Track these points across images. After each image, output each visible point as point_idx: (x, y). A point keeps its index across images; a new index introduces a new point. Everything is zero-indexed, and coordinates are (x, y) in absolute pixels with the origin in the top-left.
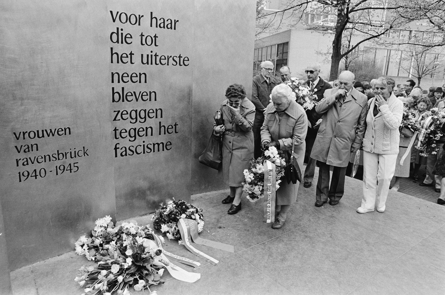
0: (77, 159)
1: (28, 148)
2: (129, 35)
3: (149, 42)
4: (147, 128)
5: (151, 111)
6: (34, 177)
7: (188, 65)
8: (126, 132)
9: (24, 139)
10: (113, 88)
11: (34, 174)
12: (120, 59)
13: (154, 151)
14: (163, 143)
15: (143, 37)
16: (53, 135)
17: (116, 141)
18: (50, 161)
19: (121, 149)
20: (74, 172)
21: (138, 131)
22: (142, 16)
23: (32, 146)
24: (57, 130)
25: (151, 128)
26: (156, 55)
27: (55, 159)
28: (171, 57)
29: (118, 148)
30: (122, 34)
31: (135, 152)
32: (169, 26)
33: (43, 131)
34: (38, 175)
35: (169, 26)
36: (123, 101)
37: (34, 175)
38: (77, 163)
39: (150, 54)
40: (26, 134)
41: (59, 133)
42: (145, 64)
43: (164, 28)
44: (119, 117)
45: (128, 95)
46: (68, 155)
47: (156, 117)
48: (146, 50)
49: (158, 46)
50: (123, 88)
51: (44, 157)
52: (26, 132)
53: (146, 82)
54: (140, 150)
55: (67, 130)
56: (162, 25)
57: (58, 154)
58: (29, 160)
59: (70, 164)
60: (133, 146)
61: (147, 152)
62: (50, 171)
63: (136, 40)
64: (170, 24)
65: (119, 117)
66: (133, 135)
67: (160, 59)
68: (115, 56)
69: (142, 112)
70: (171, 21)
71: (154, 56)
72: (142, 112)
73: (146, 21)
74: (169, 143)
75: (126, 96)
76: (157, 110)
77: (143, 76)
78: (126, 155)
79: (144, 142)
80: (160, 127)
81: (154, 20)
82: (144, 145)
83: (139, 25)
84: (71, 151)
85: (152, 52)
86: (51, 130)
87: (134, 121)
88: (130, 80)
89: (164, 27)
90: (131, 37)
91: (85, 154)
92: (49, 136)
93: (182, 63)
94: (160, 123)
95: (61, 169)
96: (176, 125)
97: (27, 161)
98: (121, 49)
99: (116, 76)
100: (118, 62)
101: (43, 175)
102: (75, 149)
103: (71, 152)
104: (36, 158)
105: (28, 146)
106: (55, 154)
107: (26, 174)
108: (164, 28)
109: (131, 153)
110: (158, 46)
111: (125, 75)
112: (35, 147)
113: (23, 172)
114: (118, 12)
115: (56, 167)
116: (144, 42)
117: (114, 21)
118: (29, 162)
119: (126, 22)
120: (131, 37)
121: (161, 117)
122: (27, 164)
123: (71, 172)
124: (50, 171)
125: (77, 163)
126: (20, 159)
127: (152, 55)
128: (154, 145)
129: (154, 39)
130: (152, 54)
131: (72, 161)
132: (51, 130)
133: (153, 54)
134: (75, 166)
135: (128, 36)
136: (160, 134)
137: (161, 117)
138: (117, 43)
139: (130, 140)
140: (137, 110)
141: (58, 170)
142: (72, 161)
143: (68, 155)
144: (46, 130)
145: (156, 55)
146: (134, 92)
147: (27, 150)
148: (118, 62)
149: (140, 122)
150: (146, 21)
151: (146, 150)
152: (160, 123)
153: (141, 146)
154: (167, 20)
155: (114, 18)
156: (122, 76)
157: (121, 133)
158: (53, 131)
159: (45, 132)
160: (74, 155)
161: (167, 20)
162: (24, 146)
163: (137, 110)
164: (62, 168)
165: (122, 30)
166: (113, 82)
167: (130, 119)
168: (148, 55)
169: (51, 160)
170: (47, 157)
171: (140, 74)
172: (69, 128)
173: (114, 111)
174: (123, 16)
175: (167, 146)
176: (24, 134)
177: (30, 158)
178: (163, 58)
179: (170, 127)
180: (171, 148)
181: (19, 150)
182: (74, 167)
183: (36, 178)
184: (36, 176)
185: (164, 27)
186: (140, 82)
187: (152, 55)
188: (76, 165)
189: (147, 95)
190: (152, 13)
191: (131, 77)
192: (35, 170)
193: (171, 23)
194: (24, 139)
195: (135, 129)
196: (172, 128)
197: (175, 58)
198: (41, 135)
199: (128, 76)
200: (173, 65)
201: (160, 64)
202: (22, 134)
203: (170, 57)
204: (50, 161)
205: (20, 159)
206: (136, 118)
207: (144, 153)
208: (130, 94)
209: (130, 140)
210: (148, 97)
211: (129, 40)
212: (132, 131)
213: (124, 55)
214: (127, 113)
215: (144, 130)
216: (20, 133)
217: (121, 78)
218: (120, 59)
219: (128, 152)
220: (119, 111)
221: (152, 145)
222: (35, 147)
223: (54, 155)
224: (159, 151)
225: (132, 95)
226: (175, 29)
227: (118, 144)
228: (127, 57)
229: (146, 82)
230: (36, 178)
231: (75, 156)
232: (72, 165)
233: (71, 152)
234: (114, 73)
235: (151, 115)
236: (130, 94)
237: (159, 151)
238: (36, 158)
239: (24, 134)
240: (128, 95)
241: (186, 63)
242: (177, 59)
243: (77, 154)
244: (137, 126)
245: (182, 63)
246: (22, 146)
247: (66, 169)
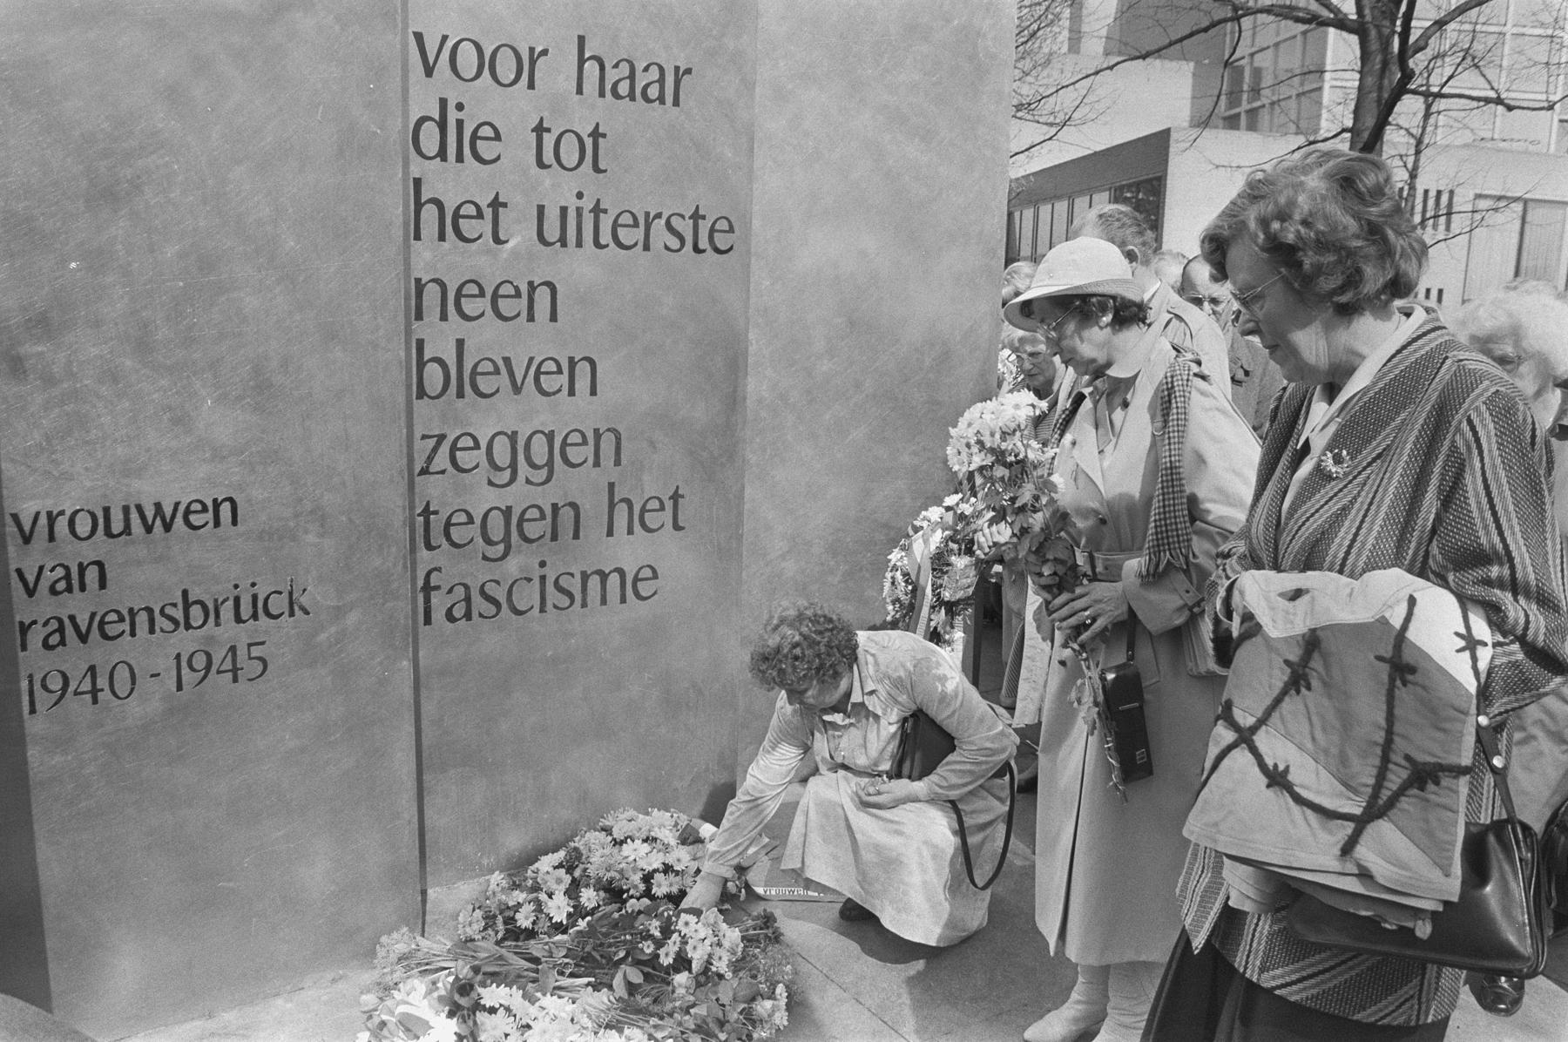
1: (68, 577)
2: (487, 128)
3: (570, 156)
5: (575, 438)
6: (88, 697)
7: (731, 248)
8: (471, 520)
9: (52, 538)
10: (420, 344)
11: (86, 686)
12: (452, 224)
13: (584, 605)
14: (621, 572)
15: (545, 135)
16: (167, 527)
18: (152, 631)
19: (450, 591)
20: (249, 680)
21: (521, 520)
22: (545, 52)
23: (82, 569)
24: (182, 508)
25: (573, 505)
26: (597, 210)
27: (169, 626)
28: (659, 216)
29: (437, 588)
30: (460, 123)
31: (505, 606)
32: (653, 92)
33: (126, 510)
34: (102, 690)
35: (653, 92)
36: (460, 394)
37: (90, 689)
38: (263, 643)
39: (572, 203)
40: (60, 518)
41: (192, 518)
42: (554, 244)
43: (633, 98)
44: (442, 460)
45: (479, 370)
46: (227, 611)
47: (597, 464)
48: (559, 190)
49: (605, 171)
50: (460, 344)
51: (127, 618)
52: (62, 513)
53: (554, 318)
54: (527, 596)
55: (226, 509)
56: (623, 89)
57: (187, 606)
58: (67, 622)
59: (233, 649)
60: (498, 582)
61: (555, 607)
62: (152, 676)
63: (517, 150)
64: (657, 85)
65: (442, 460)
66: (497, 533)
67: (615, 225)
68: (429, 213)
69: (540, 445)
70: (661, 69)
71: (590, 212)
72: (540, 445)
73: (557, 74)
74: (647, 573)
75: (474, 373)
77: (543, 296)
78: (468, 616)
79: (543, 564)
80: (612, 506)
81: (591, 68)
82: (543, 578)
83: (531, 86)
84: (236, 592)
85: (580, 196)
86: (158, 506)
87: (507, 474)
89: (632, 97)
90: (498, 137)
91: (296, 608)
92: (149, 529)
94: (611, 486)
95: (195, 666)
96: (676, 497)
97: (61, 629)
99: (432, 294)
100: (442, 237)
101: (122, 686)
102: (253, 585)
103: (237, 600)
104: (97, 619)
105: (67, 568)
106: (175, 605)
107: (56, 684)
108: (633, 98)
110: (605, 171)
112: (92, 575)
113: (45, 676)
114: (445, 38)
115: (178, 657)
117: (429, 71)
118: (67, 632)
119: (479, 74)
120: (498, 137)
121: (618, 462)
122: (63, 642)
123: (235, 680)
124: (152, 676)
125: (263, 643)
126: (34, 622)
127: (579, 211)
128: (585, 577)
129: (589, 142)
130: (580, 203)
132: (158, 506)
133: (587, 204)
134: (252, 655)
135: (486, 131)
136: (610, 533)
137: (618, 462)
138: (439, 159)
139: (485, 558)
140: (515, 433)
141: (183, 672)
142: (239, 635)
143: (227, 611)
144: (139, 508)
145: (597, 210)
146: (507, 360)
147: (61, 586)
148: (442, 237)
149: (528, 481)
150: (557, 74)
151: (553, 596)
152: (611, 486)
153: (529, 580)
154: (646, 69)
155: (431, 63)
156: (459, 295)
157: (448, 524)
158: (168, 511)
159: (133, 510)
160: (250, 612)
161: (646, 69)
162: (52, 570)
163: (515, 433)
164: (200, 661)
165: (460, 107)
168: (564, 210)
169: (157, 629)
170: (142, 618)
171: (532, 287)
172: (231, 500)
173: (424, 437)
174: (467, 51)
175: (640, 585)
176: (52, 519)
177: (72, 618)
178: (626, 219)
179: (654, 504)
180: (655, 593)
181: (31, 585)
182: (250, 658)
183: (95, 701)
184: (94, 692)
185: (632, 97)
186: (531, 318)
187: (579, 211)
188: (255, 652)
189: (560, 371)
190: (581, 39)
191: (495, 296)
192: (92, 669)
193: (661, 81)
194: (52, 538)
195: (507, 512)
196: (662, 508)
197: (675, 222)
198: (117, 526)
199: (482, 294)
200: (667, 248)
201: (612, 245)
202: (43, 520)
203: (653, 219)
204: (152, 631)
205: (34, 622)
206: (513, 466)
207: (542, 610)
208: (487, 367)
209: (485, 558)
210: (564, 379)
212: (496, 520)
213: (471, 210)
214: (477, 446)
215: (543, 517)
216: (38, 514)
217: (454, 301)
218: (452, 224)
219: (479, 603)
220: (442, 437)
221: (578, 577)
222: (92, 575)
223: (169, 611)
224: (604, 601)
225: (497, 372)
226: (676, 103)
227: (434, 575)
228: (480, 215)
229: (554, 318)
230: (95, 701)
231: (255, 616)
232: (242, 653)
233: (237, 600)
234: (423, 282)
235: (574, 454)
236: (489, 367)
237: (604, 601)
238: (97, 619)
239: (52, 519)
240: (479, 370)
241: (722, 241)
242: (685, 227)
243: (259, 608)
244: (518, 496)
246: (41, 568)
247: (214, 669)
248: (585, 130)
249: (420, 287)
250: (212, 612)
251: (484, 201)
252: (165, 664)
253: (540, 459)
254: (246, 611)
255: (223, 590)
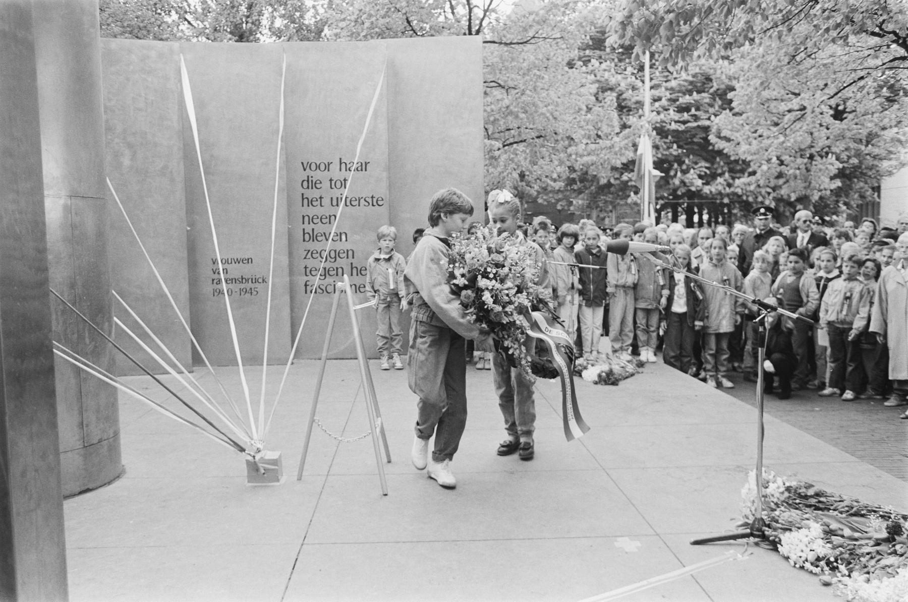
0: (257, 285)
4: (337, 268)
5: (342, 251)
10: (304, 230)
14: (355, 285)
17: (306, 278)
21: (329, 271)
25: (342, 268)
32: (359, 169)
35: (359, 169)
36: (313, 241)
39: (340, 196)
44: (309, 255)
46: (250, 281)
47: (348, 258)
50: (313, 229)
55: (250, 260)
65: (309, 255)
67: (351, 201)
68: (306, 201)
73: (335, 167)
75: (316, 236)
76: (348, 251)
80: (352, 268)
81: (343, 166)
88: (320, 223)
93: (375, 204)
94: (352, 264)
98: (312, 194)
99: (306, 219)
107: (218, 291)
109: (321, 291)
111: (315, 217)
116: (333, 186)
117: (305, 170)
121: (353, 258)
129: (343, 182)
131: (253, 286)
137: (353, 258)
142: (253, 286)
143: (250, 281)
152: (352, 264)
157: (311, 271)
166: (303, 223)
167: (320, 258)
168: (337, 198)
171: (330, 216)
178: (354, 199)
190: (340, 159)
191: (321, 219)
193: (362, 166)
197: (367, 199)
208: (319, 235)
211: (318, 186)
213: (315, 199)
217: (311, 220)
218: (310, 203)
220: (309, 251)
226: (366, 170)
241: (380, 203)
242: (370, 200)
243: (257, 281)
245: (375, 204)
248: (342, 180)
249: (303, 217)
250: (247, 280)
251: (318, 197)
252: (238, 290)
253: (333, 255)
254: (254, 281)
255: (250, 277)
